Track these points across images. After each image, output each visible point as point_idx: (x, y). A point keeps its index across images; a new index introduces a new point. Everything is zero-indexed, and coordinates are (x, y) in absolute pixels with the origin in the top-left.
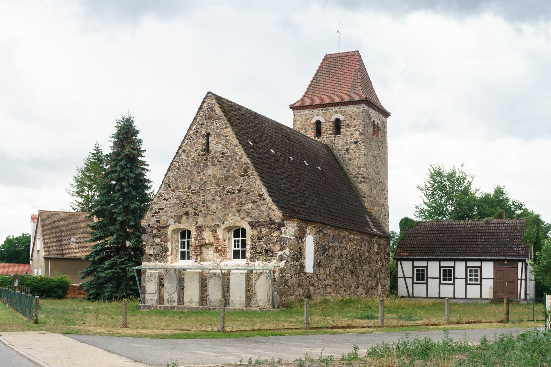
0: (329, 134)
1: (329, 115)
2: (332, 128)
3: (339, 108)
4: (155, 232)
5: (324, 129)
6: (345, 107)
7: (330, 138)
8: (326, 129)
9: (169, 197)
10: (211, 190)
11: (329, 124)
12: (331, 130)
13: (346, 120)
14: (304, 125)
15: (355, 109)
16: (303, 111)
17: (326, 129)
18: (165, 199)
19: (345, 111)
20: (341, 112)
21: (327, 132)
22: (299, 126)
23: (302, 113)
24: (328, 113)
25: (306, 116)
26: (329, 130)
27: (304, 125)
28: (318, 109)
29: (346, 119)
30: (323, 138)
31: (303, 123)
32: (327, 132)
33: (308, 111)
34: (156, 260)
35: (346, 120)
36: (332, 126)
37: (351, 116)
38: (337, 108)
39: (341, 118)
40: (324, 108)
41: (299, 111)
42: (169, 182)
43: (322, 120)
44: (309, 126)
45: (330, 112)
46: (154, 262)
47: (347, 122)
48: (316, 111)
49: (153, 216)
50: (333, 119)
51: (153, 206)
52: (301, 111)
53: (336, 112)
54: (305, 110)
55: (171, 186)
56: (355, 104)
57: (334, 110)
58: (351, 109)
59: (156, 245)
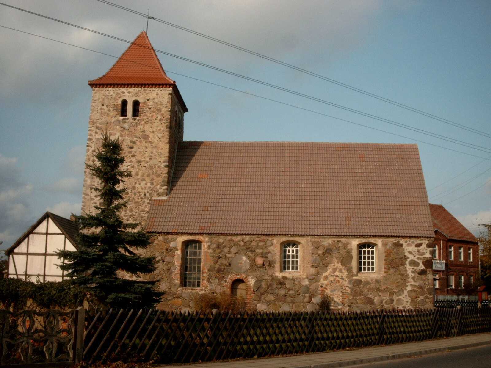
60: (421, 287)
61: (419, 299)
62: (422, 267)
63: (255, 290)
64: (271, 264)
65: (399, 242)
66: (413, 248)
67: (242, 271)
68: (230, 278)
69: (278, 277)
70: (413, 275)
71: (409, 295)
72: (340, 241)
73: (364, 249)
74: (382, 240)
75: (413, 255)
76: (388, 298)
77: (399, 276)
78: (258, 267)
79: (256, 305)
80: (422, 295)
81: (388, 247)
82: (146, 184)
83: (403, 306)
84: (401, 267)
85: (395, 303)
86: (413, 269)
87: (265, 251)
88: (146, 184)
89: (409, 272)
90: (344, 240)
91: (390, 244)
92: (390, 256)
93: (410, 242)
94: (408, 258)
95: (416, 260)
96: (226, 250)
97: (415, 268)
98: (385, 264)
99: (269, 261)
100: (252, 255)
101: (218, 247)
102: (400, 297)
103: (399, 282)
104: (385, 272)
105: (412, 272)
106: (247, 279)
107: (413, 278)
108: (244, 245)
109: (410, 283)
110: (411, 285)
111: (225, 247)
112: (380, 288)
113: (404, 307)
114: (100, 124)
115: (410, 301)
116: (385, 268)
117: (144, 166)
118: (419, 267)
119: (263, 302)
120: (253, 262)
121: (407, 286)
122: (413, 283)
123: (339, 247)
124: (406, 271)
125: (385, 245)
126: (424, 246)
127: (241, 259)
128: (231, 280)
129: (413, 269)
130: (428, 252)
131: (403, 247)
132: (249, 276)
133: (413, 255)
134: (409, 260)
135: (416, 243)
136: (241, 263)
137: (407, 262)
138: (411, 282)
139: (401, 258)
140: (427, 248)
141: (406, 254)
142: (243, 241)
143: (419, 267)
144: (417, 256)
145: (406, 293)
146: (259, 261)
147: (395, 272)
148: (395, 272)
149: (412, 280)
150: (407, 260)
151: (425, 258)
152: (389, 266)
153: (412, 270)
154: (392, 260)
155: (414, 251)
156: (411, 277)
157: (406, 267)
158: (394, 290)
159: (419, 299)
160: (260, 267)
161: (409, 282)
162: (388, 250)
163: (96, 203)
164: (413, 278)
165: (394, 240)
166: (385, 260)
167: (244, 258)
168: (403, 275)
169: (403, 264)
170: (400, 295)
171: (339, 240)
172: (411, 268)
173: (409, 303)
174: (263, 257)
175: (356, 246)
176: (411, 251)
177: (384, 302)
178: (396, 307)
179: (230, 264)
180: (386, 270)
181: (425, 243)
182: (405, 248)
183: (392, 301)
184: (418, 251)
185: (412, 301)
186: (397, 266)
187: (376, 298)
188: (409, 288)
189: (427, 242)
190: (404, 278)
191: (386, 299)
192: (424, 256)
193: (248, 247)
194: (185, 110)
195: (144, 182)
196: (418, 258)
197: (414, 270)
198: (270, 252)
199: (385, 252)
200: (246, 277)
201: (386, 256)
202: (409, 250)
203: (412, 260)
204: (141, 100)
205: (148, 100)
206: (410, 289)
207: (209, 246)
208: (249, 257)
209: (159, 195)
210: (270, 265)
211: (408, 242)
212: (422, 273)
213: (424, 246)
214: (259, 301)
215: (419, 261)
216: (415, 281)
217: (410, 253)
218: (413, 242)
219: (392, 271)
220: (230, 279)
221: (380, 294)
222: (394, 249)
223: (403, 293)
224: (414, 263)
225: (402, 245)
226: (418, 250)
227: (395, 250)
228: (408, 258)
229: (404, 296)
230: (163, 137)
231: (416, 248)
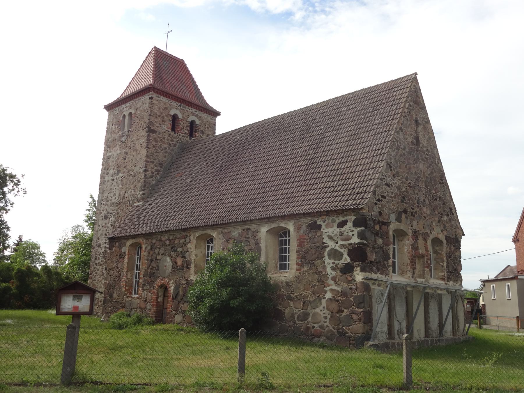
0: (185, 133)
1: (187, 114)
2: (188, 128)
3: (196, 112)
4: (377, 227)
5: (181, 126)
6: (200, 112)
7: (185, 138)
8: (183, 127)
9: (391, 183)
10: (423, 189)
11: (186, 123)
12: (187, 130)
13: (201, 126)
14: (161, 113)
15: (209, 118)
16: (162, 97)
17: (183, 127)
18: (386, 184)
19: (200, 117)
20: (197, 116)
21: (184, 130)
22: (156, 112)
23: (161, 99)
24: (186, 111)
25: (165, 104)
26: (185, 130)
27: (161, 113)
28: (177, 103)
29: (201, 125)
30: (180, 135)
31: (161, 110)
32: (184, 131)
33: (167, 101)
34: (378, 270)
35: (201, 126)
36: (188, 126)
37: (205, 124)
38: (194, 110)
39: (198, 122)
40: (182, 105)
41: (158, 95)
42: (391, 163)
43: (180, 116)
44: (167, 116)
45: (188, 111)
46: (376, 274)
47: (202, 128)
48: (174, 103)
49: (376, 204)
50: (190, 120)
51: (376, 189)
52: (160, 96)
53: (193, 114)
54: (163, 97)
55: (392, 168)
56: (209, 114)
57: (191, 111)
58: (206, 117)
59: (378, 248)
60: (344, 294)
61: (344, 314)
62: (346, 259)
63: (174, 297)
64: (187, 265)
65: (315, 222)
66: (333, 230)
67: (167, 274)
68: (158, 282)
69: (192, 280)
70: (334, 273)
71: (327, 306)
72: (250, 229)
73: (285, 238)
74: (293, 222)
75: (334, 240)
76: (302, 311)
77: (316, 276)
78: (178, 270)
79: (174, 316)
80: (347, 308)
81: (302, 232)
82: (131, 192)
83: (320, 324)
84: (317, 262)
85: (310, 319)
86: (333, 263)
87: (185, 249)
88: (131, 192)
89: (329, 270)
90: (253, 227)
91: (304, 227)
92: (304, 245)
93: (330, 221)
94: (328, 246)
95: (337, 248)
96: (157, 251)
97: (336, 262)
98: (298, 258)
99: (187, 261)
100: (174, 255)
101: (151, 249)
102: (317, 310)
103: (315, 285)
104: (297, 270)
105: (333, 269)
106: (169, 285)
107: (334, 279)
108: (169, 245)
109: (330, 287)
110: (332, 290)
111: (156, 248)
112: (292, 295)
113: (322, 327)
114: (110, 143)
115: (329, 316)
116: (298, 264)
117: (131, 175)
118: (343, 261)
119: (179, 312)
120: (175, 262)
121: (326, 292)
122: (334, 287)
123: (249, 237)
124: (324, 267)
125: (298, 228)
126: (350, 224)
127: (166, 260)
128: (158, 286)
129: (333, 263)
130: (356, 235)
131: (322, 230)
132: (171, 280)
133: (334, 240)
134: (328, 249)
135: (338, 221)
136: (166, 266)
137: (326, 254)
138: (332, 285)
139: (318, 247)
140: (354, 229)
141: (324, 241)
142: (168, 239)
143: (343, 261)
144: (340, 242)
145: (324, 301)
146: (179, 261)
147: (311, 268)
148: (311, 268)
149: (332, 282)
150: (325, 250)
151: (351, 244)
152: (303, 260)
153: (332, 265)
154: (307, 252)
155: (336, 235)
156: (330, 277)
157: (324, 262)
158: (309, 299)
159: (344, 314)
160: (179, 269)
161: (329, 286)
162: (300, 236)
163: (102, 217)
164: (334, 279)
165: (308, 221)
166: (297, 252)
167: (168, 260)
168: (320, 273)
169: (321, 257)
170: (317, 307)
171: (248, 227)
172: (331, 261)
173: (328, 320)
174: (182, 257)
175: (265, 234)
176: (331, 234)
177: (296, 316)
178: (310, 325)
179: (158, 266)
180: (298, 267)
181: (350, 219)
182: (324, 231)
183: (305, 316)
184: (341, 234)
185: (331, 317)
186: (312, 261)
187: (286, 310)
188: (329, 295)
189: (354, 218)
190: (322, 279)
191: (299, 313)
192: (349, 242)
193: (172, 246)
194: (217, 114)
195: (130, 190)
196: (342, 246)
197: (334, 265)
198: (188, 251)
199: (298, 240)
200: (169, 282)
201: (298, 246)
202: (328, 234)
203: (332, 249)
204: (133, 112)
205: (137, 109)
206: (330, 297)
207: (146, 248)
208: (171, 257)
209: (138, 201)
210: (187, 267)
211: (327, 221)
212: (347, 269)
213: (350, 224)
214: (177, 310)
215: (342, 250)
216: (337, 284)
217: (330, 238)
218: (334, 221)
219: (305, 268)
220: (157, 285)
221: (292, 304)
222: (308, 234)
223: (321, 304)
224: (335, 255)
225: (320, 227)
226: (340, 232)
227: (310, 235)
228: (328, 246)
229: (321, 308)
230: (143, 142)
231: (338, 230)
